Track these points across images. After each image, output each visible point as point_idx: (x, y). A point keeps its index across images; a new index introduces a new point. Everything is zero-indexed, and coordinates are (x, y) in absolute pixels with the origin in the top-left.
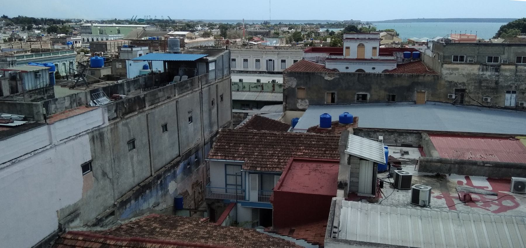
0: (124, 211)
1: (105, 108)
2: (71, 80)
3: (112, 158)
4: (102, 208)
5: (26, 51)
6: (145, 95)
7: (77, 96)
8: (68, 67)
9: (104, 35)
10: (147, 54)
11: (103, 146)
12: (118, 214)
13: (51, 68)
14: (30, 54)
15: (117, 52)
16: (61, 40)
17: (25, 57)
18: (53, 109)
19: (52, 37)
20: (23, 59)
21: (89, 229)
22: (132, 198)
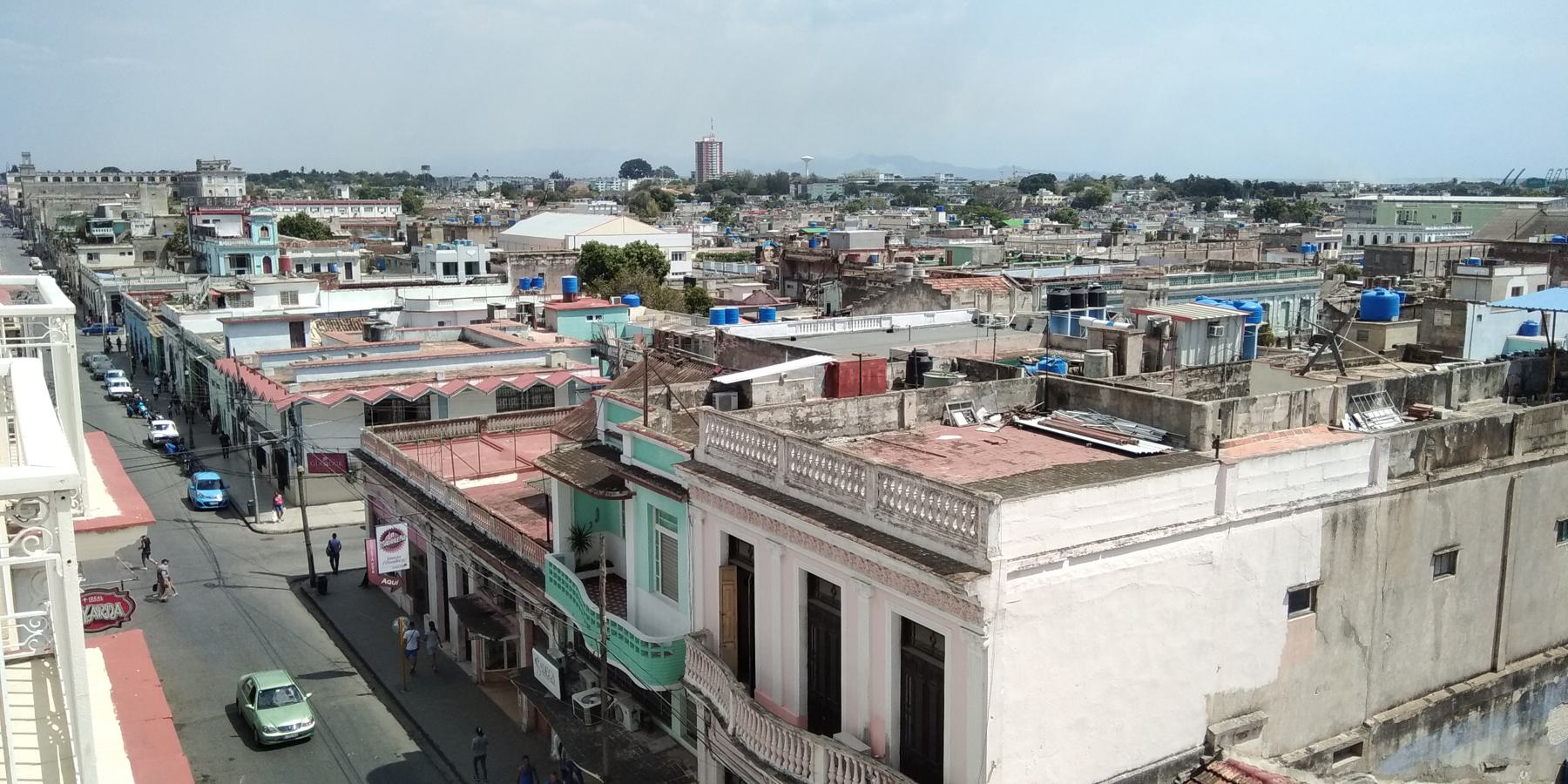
0: (1391, 751)
1: (1385, 442)
2: (1297, 349)
3: (1380, 590)
4: (1329, 725)
5: (1195, 266)
6: (1515, 416)
7: (1309, 396)
8: (1296, 315)
9: (1410, 227)
10: (1540, 288)
11: (1357, 548)
12: (1372, 755)
13: (1252, 315)
14: (1203, 273)
15: (1441, 278)
16: (1288, 238)
17: (1189, 281)
18: (1240, 424)
19: (1264, 230)
20: (1184, 287)
21: (1284, 772)
22: (1421, 720)
